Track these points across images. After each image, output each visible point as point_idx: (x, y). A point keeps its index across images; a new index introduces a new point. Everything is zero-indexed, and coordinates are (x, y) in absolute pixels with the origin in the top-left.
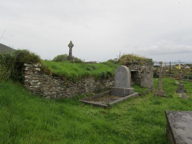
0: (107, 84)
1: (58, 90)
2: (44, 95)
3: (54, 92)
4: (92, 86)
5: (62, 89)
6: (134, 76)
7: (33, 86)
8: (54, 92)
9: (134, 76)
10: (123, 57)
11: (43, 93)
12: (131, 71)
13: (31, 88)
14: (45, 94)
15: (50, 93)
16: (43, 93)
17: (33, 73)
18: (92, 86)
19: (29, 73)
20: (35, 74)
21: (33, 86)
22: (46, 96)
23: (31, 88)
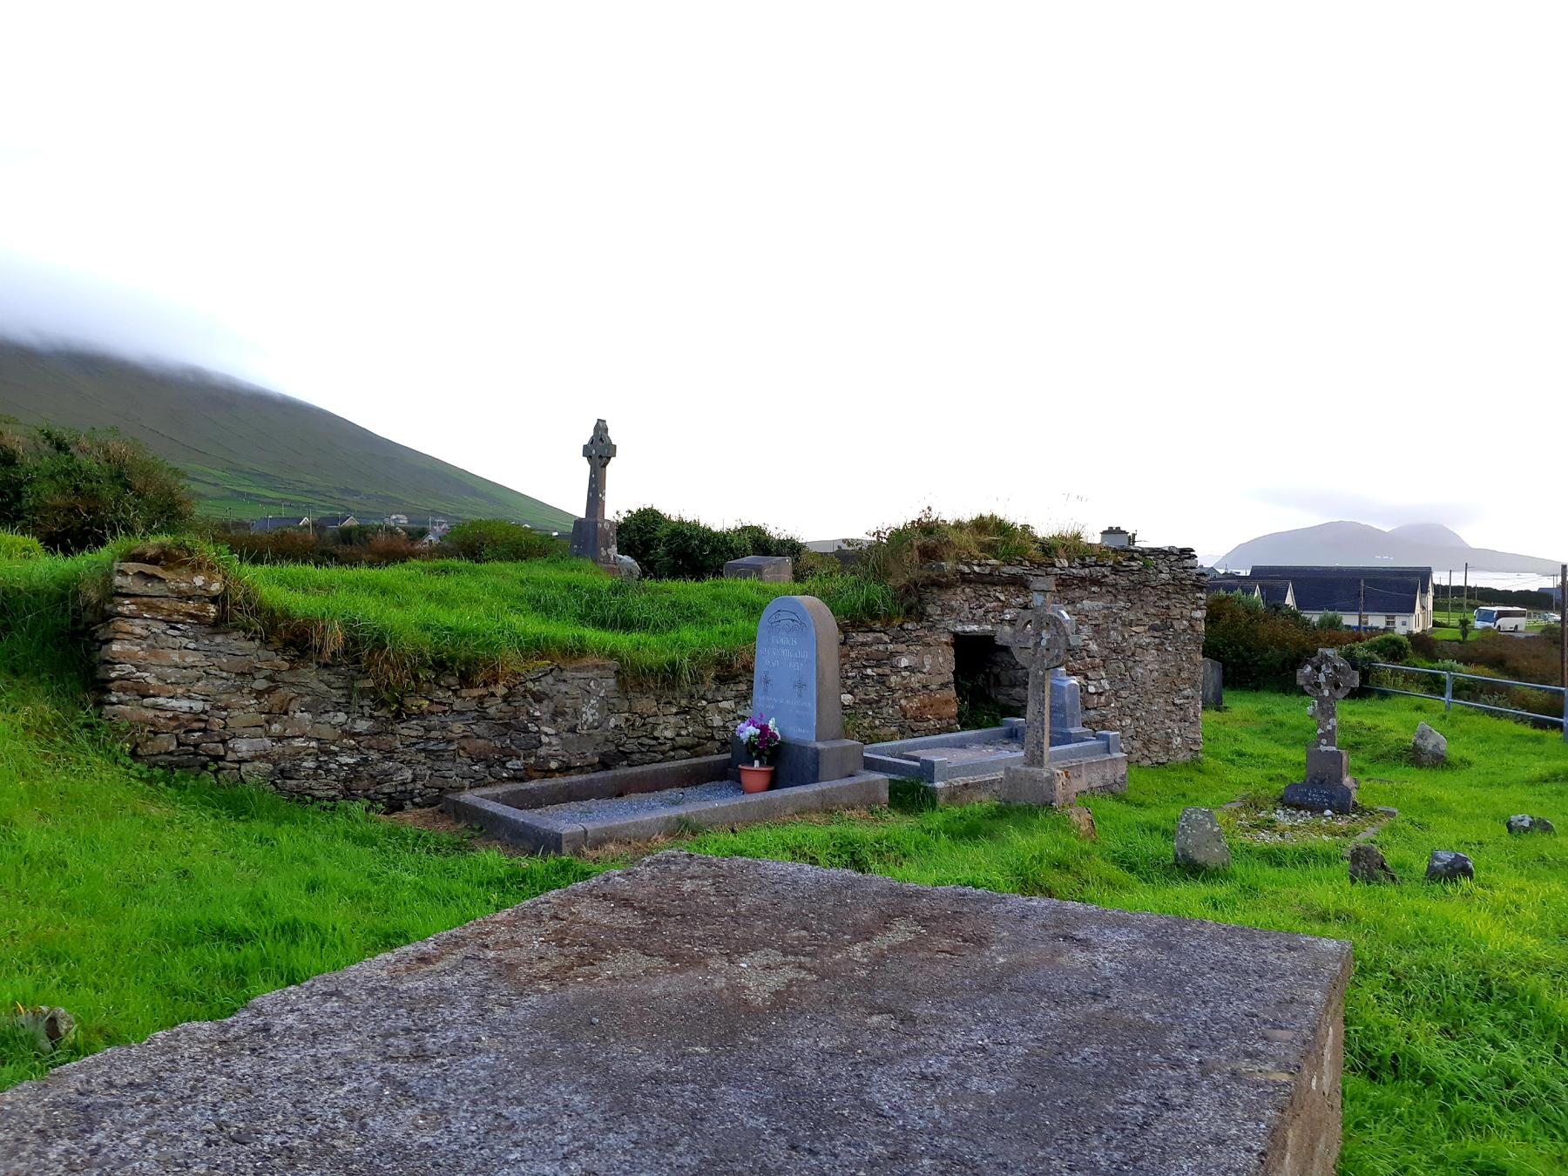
0: (720, 711)
1: (326, 732)
2: (231, 757)
3: (298, 743)
4: (589, 714)
5: (362, 725)
6: (996, 670)
7: (161, 701)
8: (298, 743)
9: (996, 670)
10: (745, 529)
11: (224, 742)
12: (956, 635)
13: (150, 714)
14: (233, 750)
15: (268, 742)
16: (224, 742)
17: (164, 626)
18: (589, 714)
19: (138, 630)
20: (176, 633)
21: (161, 701)
22: (241, 761)
23: (150, 714)
